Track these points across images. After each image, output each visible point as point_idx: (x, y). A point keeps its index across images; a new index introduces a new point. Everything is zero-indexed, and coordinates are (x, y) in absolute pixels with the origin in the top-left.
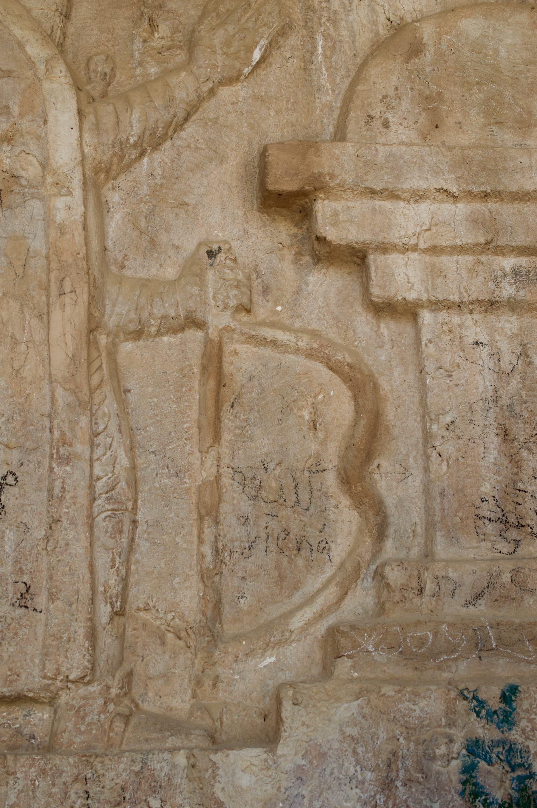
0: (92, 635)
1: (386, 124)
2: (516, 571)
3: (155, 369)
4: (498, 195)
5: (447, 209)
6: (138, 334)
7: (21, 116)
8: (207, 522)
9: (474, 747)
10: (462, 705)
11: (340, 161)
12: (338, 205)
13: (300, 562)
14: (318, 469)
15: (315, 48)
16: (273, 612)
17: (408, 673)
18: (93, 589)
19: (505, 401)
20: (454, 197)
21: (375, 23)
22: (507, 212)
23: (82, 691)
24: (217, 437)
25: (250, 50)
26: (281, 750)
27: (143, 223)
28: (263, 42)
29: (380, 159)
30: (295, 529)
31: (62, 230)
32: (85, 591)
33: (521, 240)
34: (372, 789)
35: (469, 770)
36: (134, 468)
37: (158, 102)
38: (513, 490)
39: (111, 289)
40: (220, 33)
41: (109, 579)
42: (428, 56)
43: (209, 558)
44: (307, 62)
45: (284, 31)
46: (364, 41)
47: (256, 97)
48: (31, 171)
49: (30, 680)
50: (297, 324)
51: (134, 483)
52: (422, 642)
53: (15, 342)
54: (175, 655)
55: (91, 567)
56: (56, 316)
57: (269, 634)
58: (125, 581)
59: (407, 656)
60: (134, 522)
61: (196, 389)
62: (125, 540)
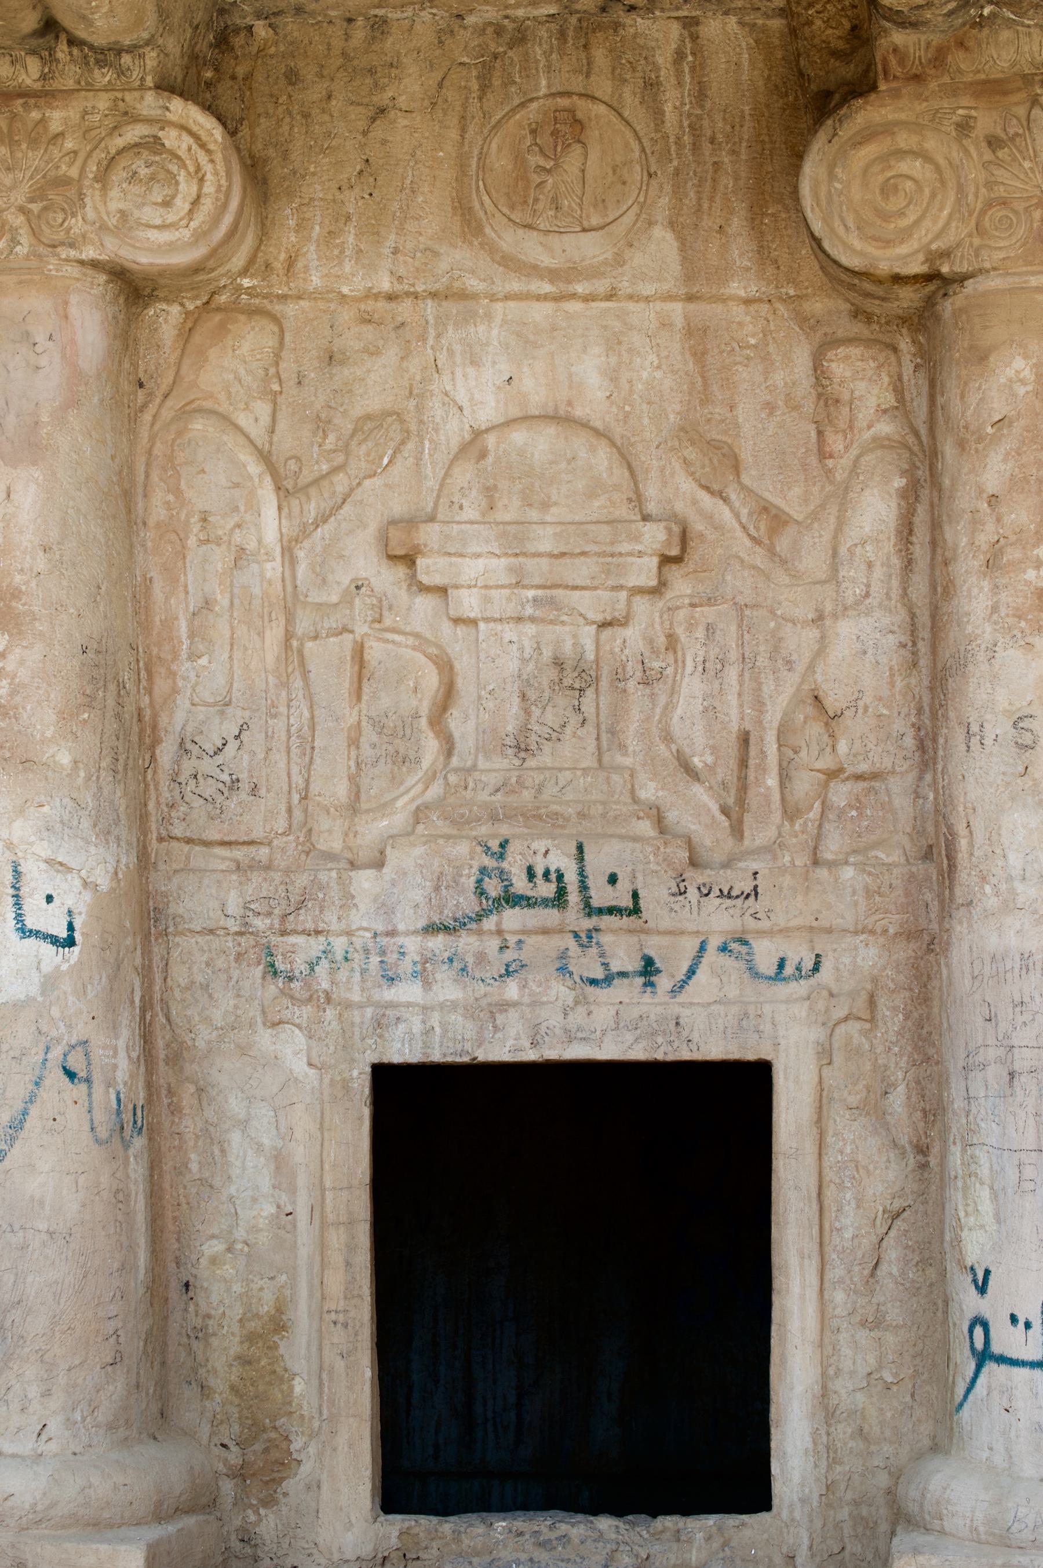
0: (290, 810)
1: (461, 508)
2: (519, 777)
3: (327, 658)
4: (525, 554)
5: (495, 561)
6: (316, 638)
7: (246, 512)
8: (353, 748)
9: (483, 870)
10: (479, 849)
11: (429, 535)
12: (429, 561)
13: (404, 769)
14: (417, 716)
15: (423, 450)
16: (388, 797)
17: (455, 832)
18: (290, 786)
19: (525, 677)
20: (499, 557)
21: (462, 430)
22: (530, 564)
23: (285, 839)
24: (359, 698)
25: (381, 458)
26: (385, 870)
27: (318, 569)
28: (390, 452)
29: (454, 533)
30: (402, 751)
31: (270, 583)
32: (286, 788)
33: (537, 581)
34: (429, 890)
35: (479, 882)
36: (313, 717)
37: (326, 495)
38: (525, 729)
39: (300, 613)
40: (364, 447)
41: (298, 780)
42: (490, 459)
43: (353, 768)
44: (419, 459)
45: (403, 443)
46: (455, 444)
47: (386, 485)
48: (252, 545)
49: (258, 834)
50: (408, 629)
51: (313, 728)
52: (463, 816)
53: (246, 649)
54: (334, 820)
55: (289, 775)
56: (268, 634)
57: (384, 808)
58: (307, 782)
59: (454, 823)
60: (313, 748)
61: (349, 670)
62: (307, 759)
